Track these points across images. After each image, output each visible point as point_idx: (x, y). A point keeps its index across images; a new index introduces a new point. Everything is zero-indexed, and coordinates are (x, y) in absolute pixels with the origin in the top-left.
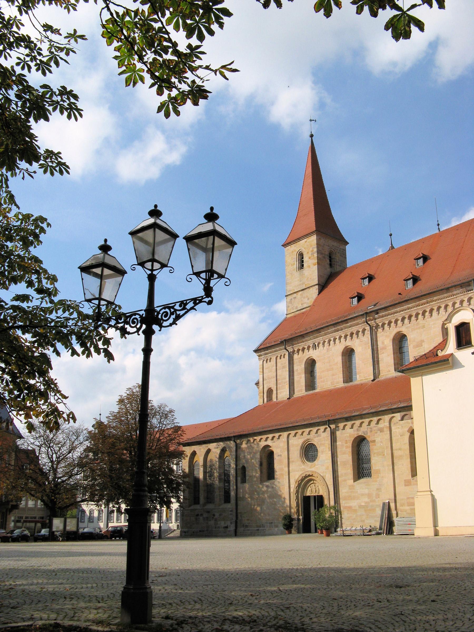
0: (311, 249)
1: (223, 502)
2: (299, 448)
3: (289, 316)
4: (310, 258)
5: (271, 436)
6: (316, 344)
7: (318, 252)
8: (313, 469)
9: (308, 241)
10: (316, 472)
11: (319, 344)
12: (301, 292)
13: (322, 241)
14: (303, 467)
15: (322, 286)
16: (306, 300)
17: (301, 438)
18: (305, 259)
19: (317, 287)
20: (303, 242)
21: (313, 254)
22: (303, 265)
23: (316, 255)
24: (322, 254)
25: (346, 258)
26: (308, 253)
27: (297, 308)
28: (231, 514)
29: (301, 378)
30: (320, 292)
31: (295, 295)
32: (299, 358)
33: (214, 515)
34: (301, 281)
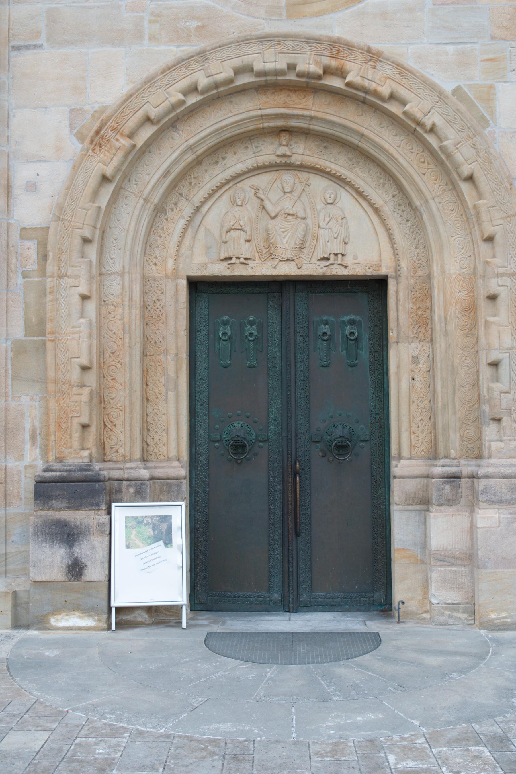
10: (373, 56)
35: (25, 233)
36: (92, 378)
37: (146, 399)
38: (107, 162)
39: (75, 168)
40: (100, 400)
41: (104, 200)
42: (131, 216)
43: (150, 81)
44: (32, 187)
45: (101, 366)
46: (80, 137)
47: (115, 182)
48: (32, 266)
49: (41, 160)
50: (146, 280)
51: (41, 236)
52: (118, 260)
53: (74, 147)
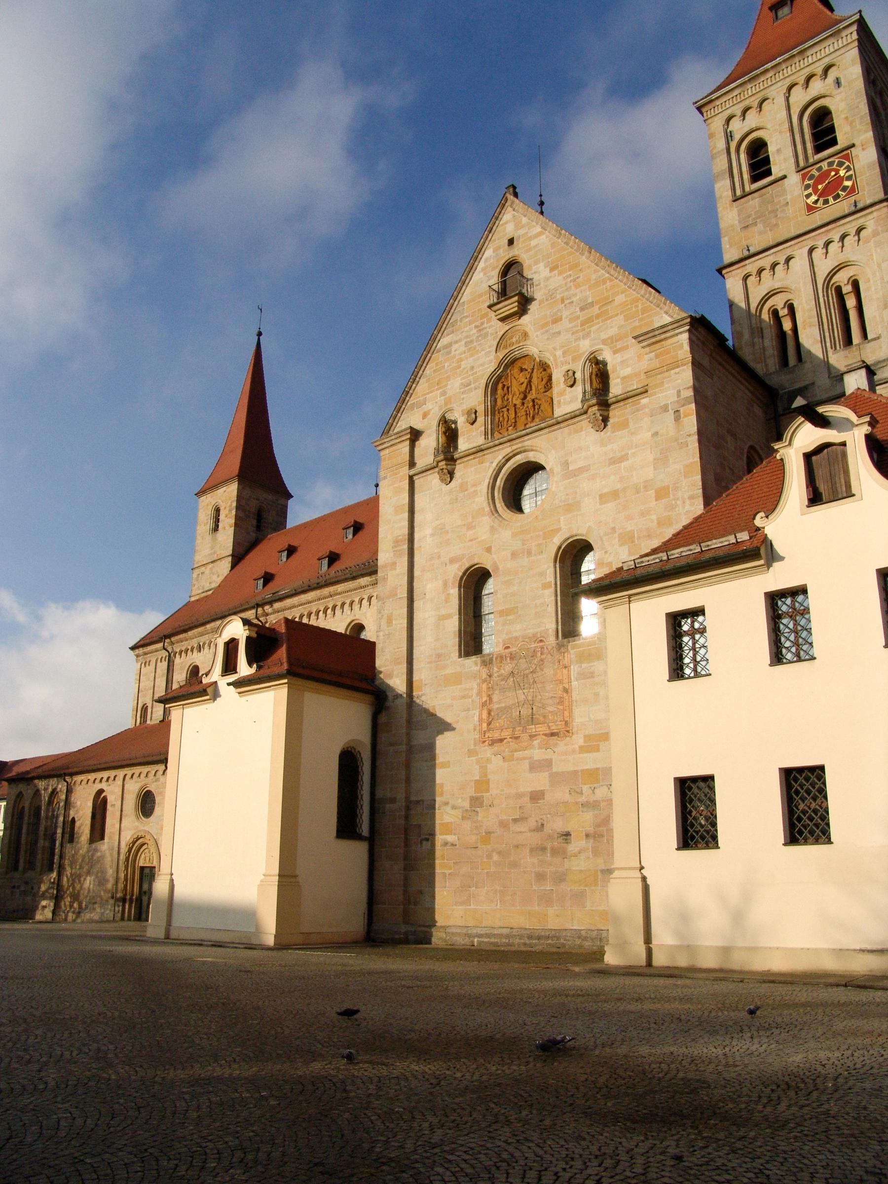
3: (193, 599)
7: (237, 508)
8: (146, 828)
11: (204, 644)
12: (211, 565)
13: (247, 492)
14: (136, 824)
15: (237, 558)
16: (215, 578)
18: (222, 517)
19: (230, 558)
21: (230, 511)
22: (218, 526)
23: (234, 512)
24: (244, 511)
25: (285, 518)
30: (233, 567)
31: (203, 569)
32: (182, 663)
33: (32, 888)
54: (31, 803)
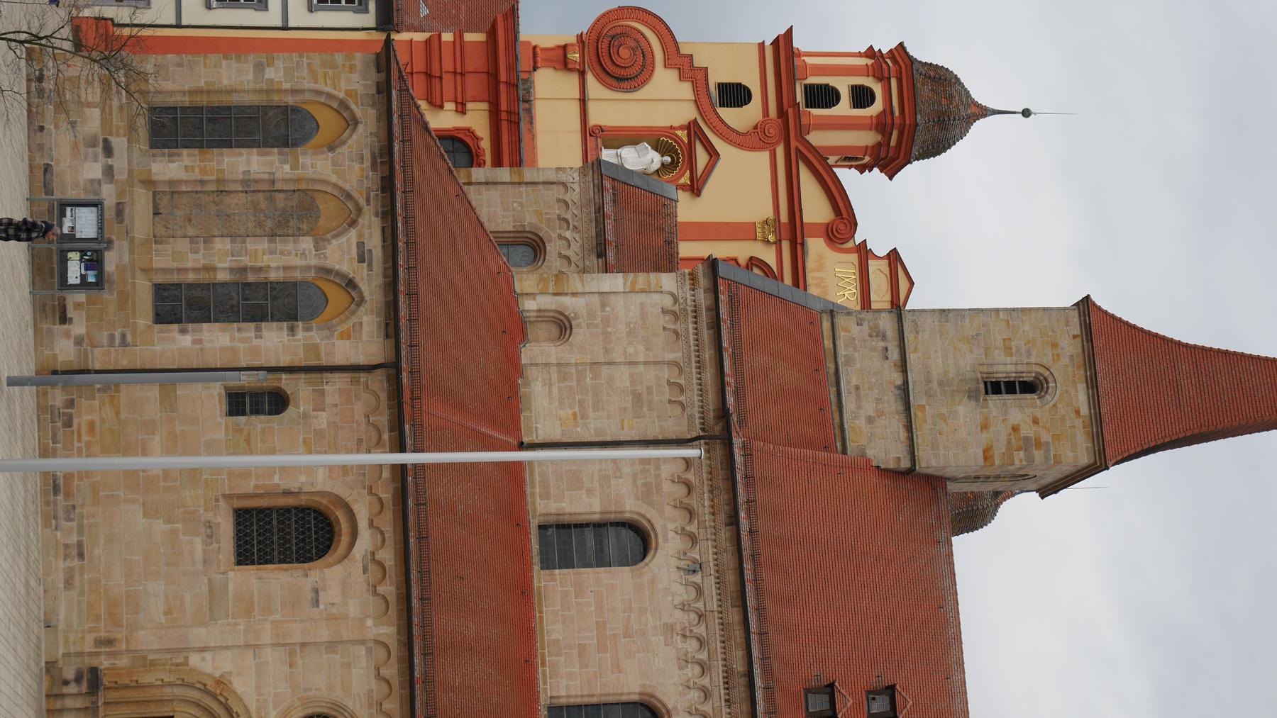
0: (1045, 437)
1: (159, 279)
2: (338, 695)
4: (1015, 429)
5: (388, 556)
6: (697, 578)
9: (1079, 423)
16: (869, 408)
17: (370, 705)
20: (1081, 398)
26: (1036, 421)
27: (849, 361)
28: (112, 337)
29: (590, 492)
31: (894, 355)
32: (658, 486)
34: (940, 383)
35: (186, 658)
36: (134, 684)
37: (127, 703)
38: (211, 686)
39: (209, 675)
40: (126, 687)
41: (198, 685)
42: (194, 695)
43: (241, 700)
44: (203, 659)
45: (139, 686)
46: (221, 676)
47: (205, 690)
48: (174, 661)
49: (213, 660)
50: (172, 700)
51: (186, 663)
52: (178, 691)
53: (217, 674)
54: (326, 182)
